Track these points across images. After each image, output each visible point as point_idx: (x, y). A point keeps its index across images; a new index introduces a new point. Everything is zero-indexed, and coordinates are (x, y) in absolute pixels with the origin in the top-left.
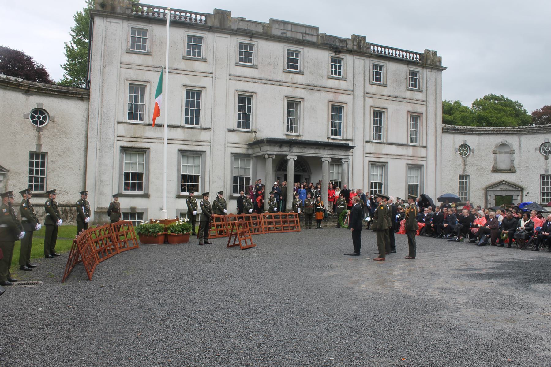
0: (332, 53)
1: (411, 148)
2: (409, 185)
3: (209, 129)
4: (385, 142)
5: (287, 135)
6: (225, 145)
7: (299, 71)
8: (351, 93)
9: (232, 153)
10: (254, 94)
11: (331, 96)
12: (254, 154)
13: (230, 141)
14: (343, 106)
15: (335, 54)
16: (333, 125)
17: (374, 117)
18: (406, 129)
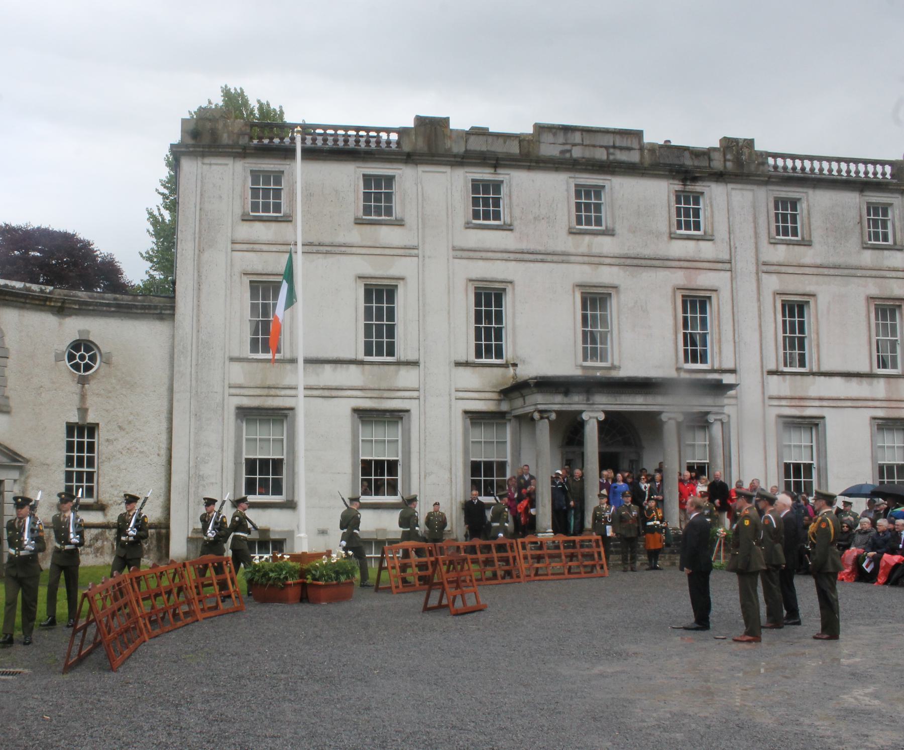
0: (676, 182)
3: (416, 364)
4: (815, 369)
5: (584, 368)
6: (450, 395)
7: (603, 228)
8: (727, 266)
10: (509, 284)
11: (679, 278)
15: (685, 185)
17: (784, 315)
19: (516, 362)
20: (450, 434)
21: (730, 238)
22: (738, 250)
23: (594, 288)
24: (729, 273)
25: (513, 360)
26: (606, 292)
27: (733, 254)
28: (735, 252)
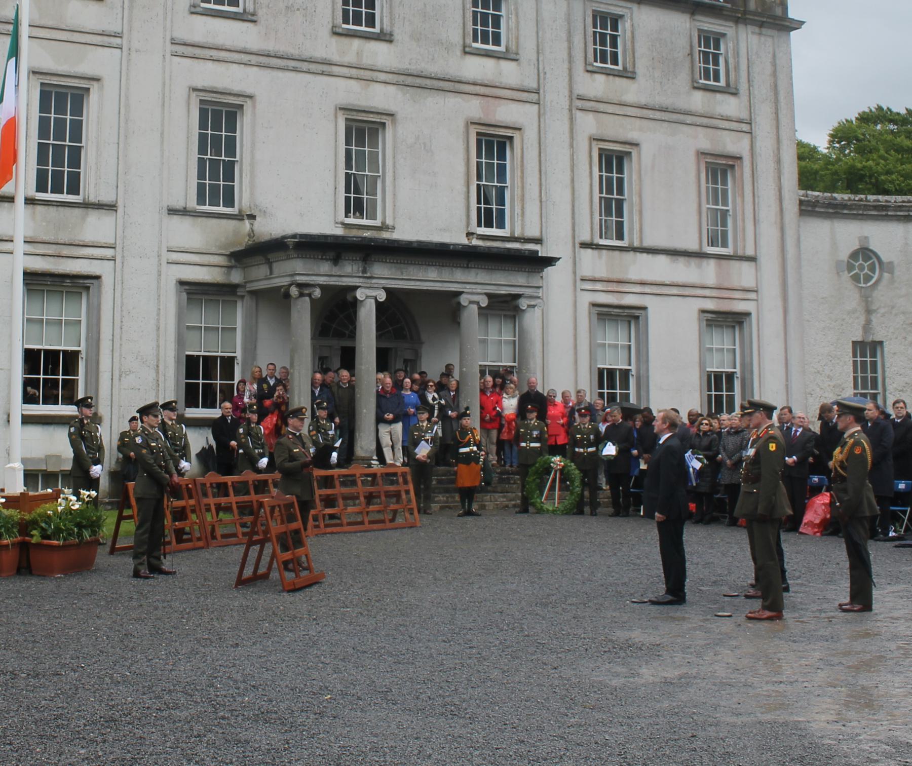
1: (712, 262)
3: (111, 207)
4: (636, 244)
5: (346, 226)
7: (377, 30)
8: (534, 97)
9: (182, 283)
10: (247, 100)
11: (474, 108)
12: (248, 285)
13: (176, 243)
14: (511, 138)
16: (483, 195)
17: (600, 170)
18: (695, 206)
19: (253, 212)
20: (158, 314)
21: (538, 60)
22: (548, 76)
23: (363, 114)
24: (536, 106)
25: (251, 211)
26: (379, 120)
27: (541, 81)
28: (545, 79)
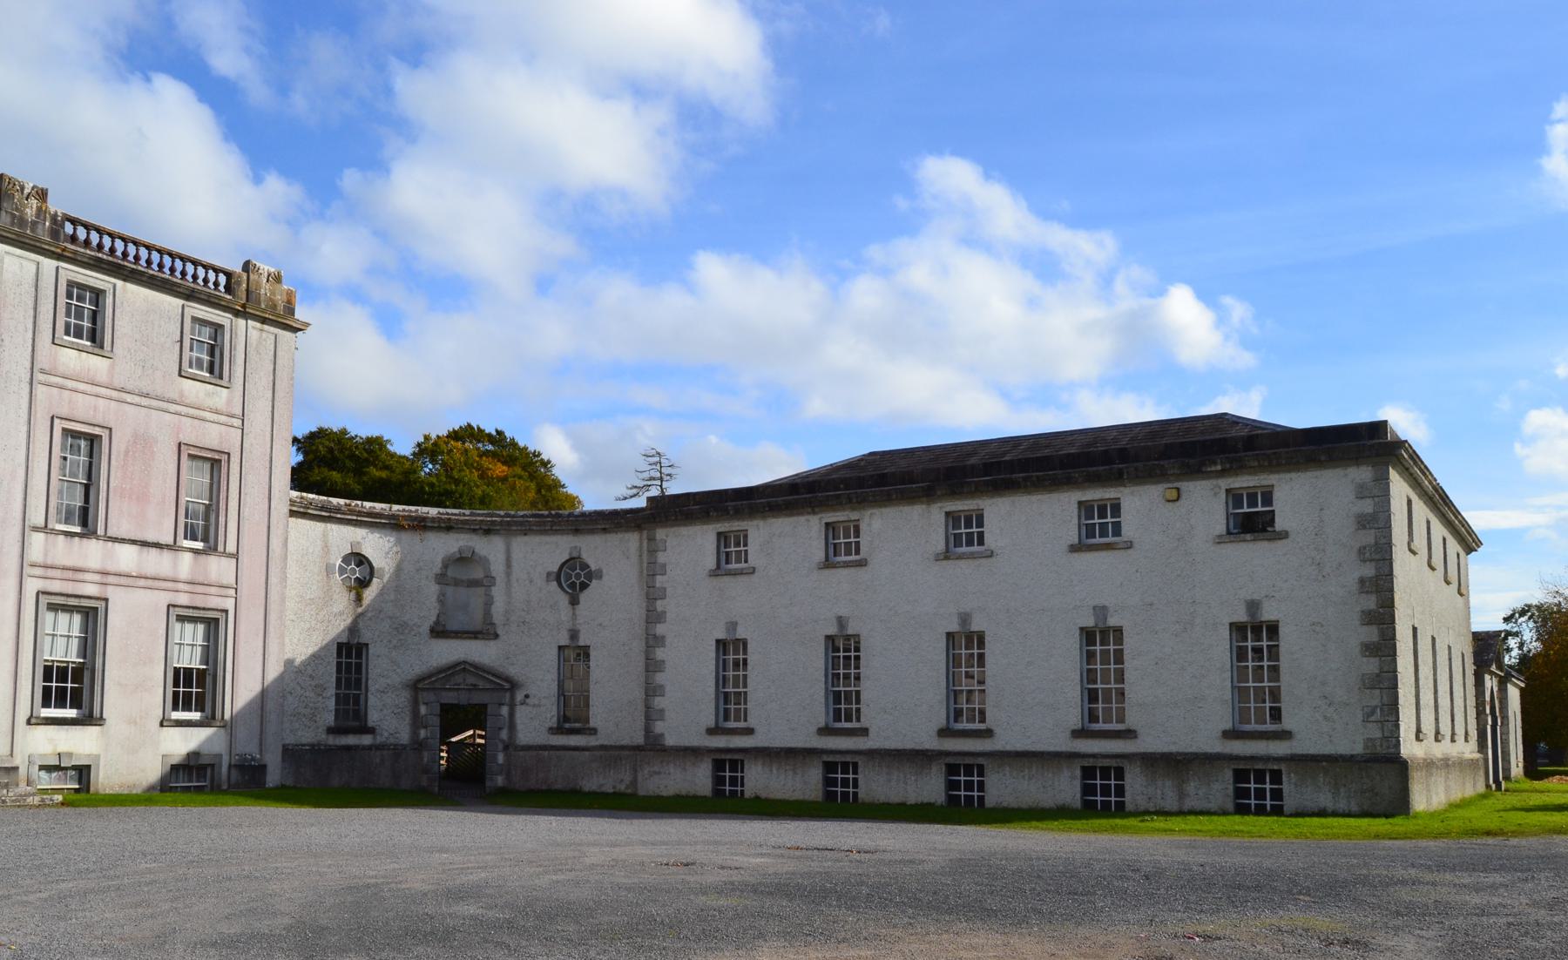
2: (177, 671)
